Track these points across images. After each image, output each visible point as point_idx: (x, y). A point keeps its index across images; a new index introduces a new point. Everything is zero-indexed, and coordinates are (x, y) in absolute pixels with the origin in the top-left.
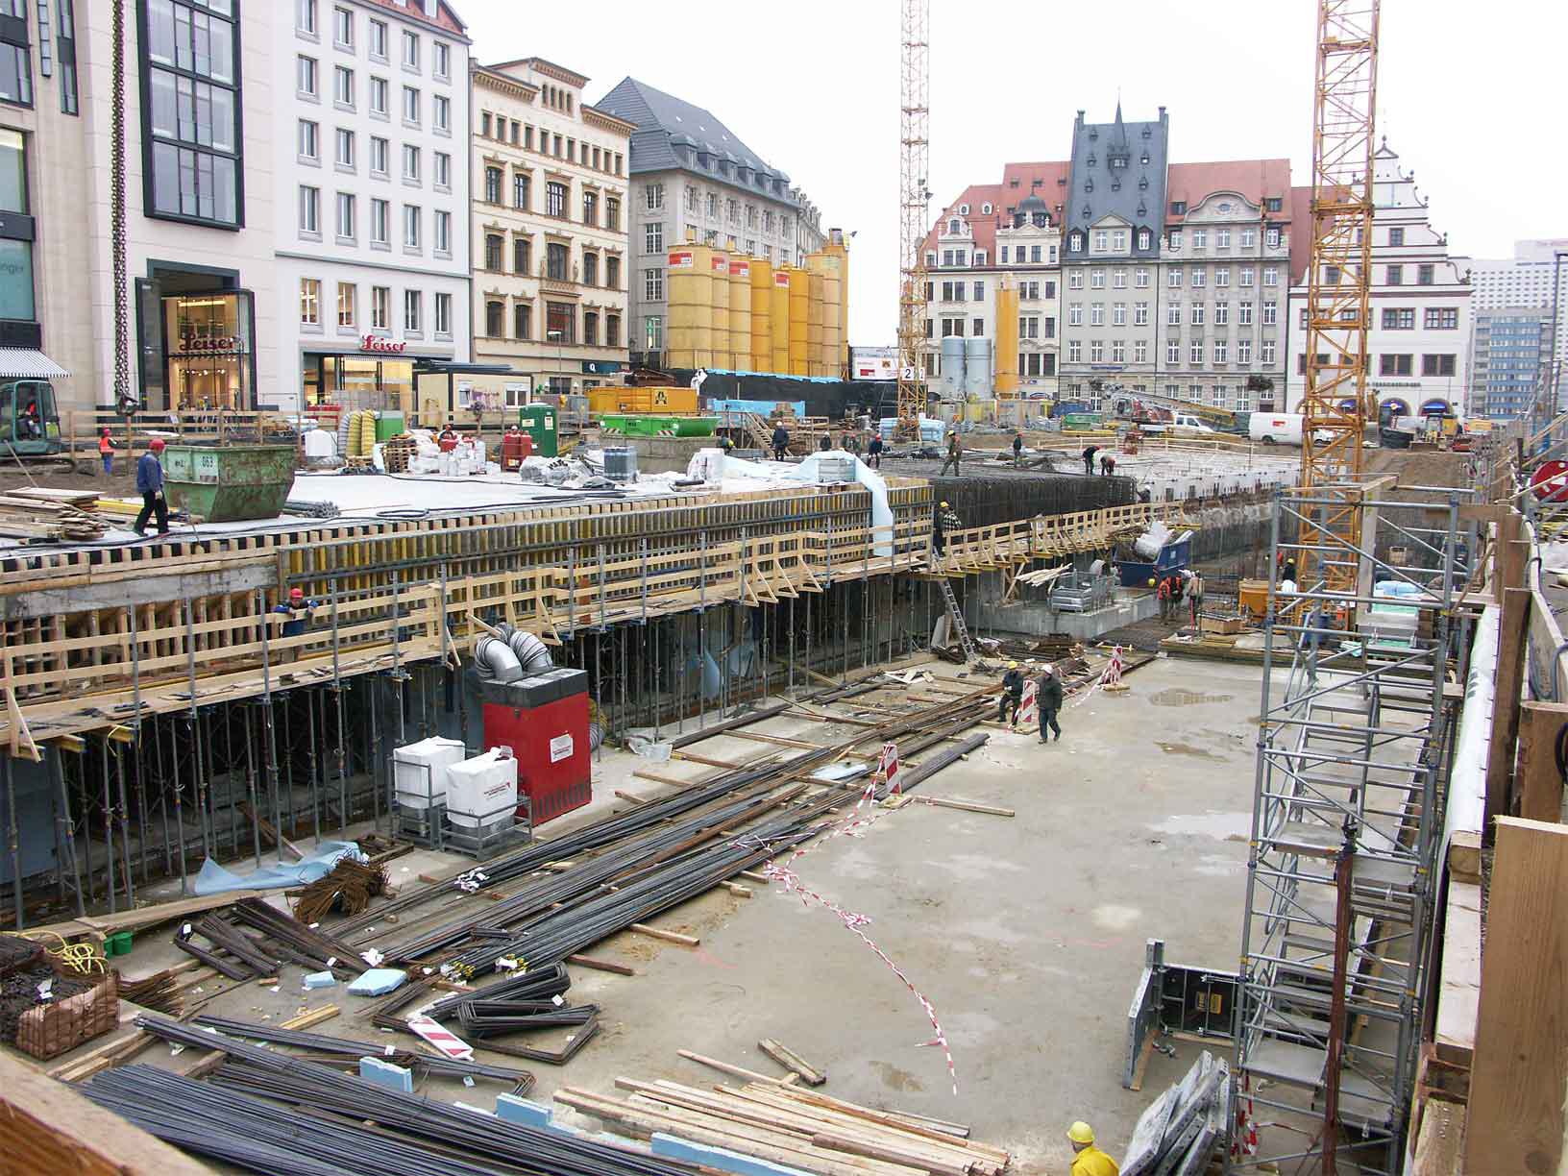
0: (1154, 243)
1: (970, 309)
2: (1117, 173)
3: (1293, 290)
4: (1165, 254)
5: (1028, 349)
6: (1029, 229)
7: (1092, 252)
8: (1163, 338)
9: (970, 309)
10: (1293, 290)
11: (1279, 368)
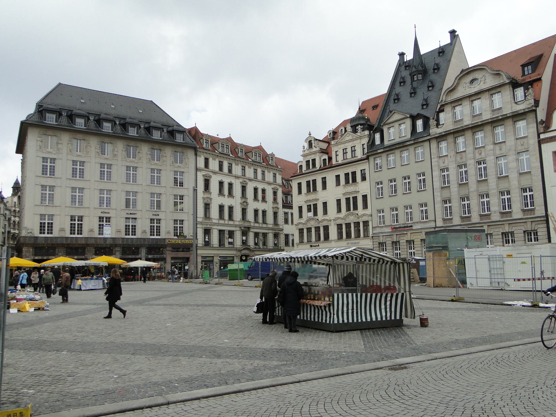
0: (426, 126)
2: (415, 84)
3: (542, 136)
4: (434, 131)
5: (352, 219)
6: (350, 136)
7: (386, 143)
8: (438, 199)
9: (321, 196)
10: (542, 136)
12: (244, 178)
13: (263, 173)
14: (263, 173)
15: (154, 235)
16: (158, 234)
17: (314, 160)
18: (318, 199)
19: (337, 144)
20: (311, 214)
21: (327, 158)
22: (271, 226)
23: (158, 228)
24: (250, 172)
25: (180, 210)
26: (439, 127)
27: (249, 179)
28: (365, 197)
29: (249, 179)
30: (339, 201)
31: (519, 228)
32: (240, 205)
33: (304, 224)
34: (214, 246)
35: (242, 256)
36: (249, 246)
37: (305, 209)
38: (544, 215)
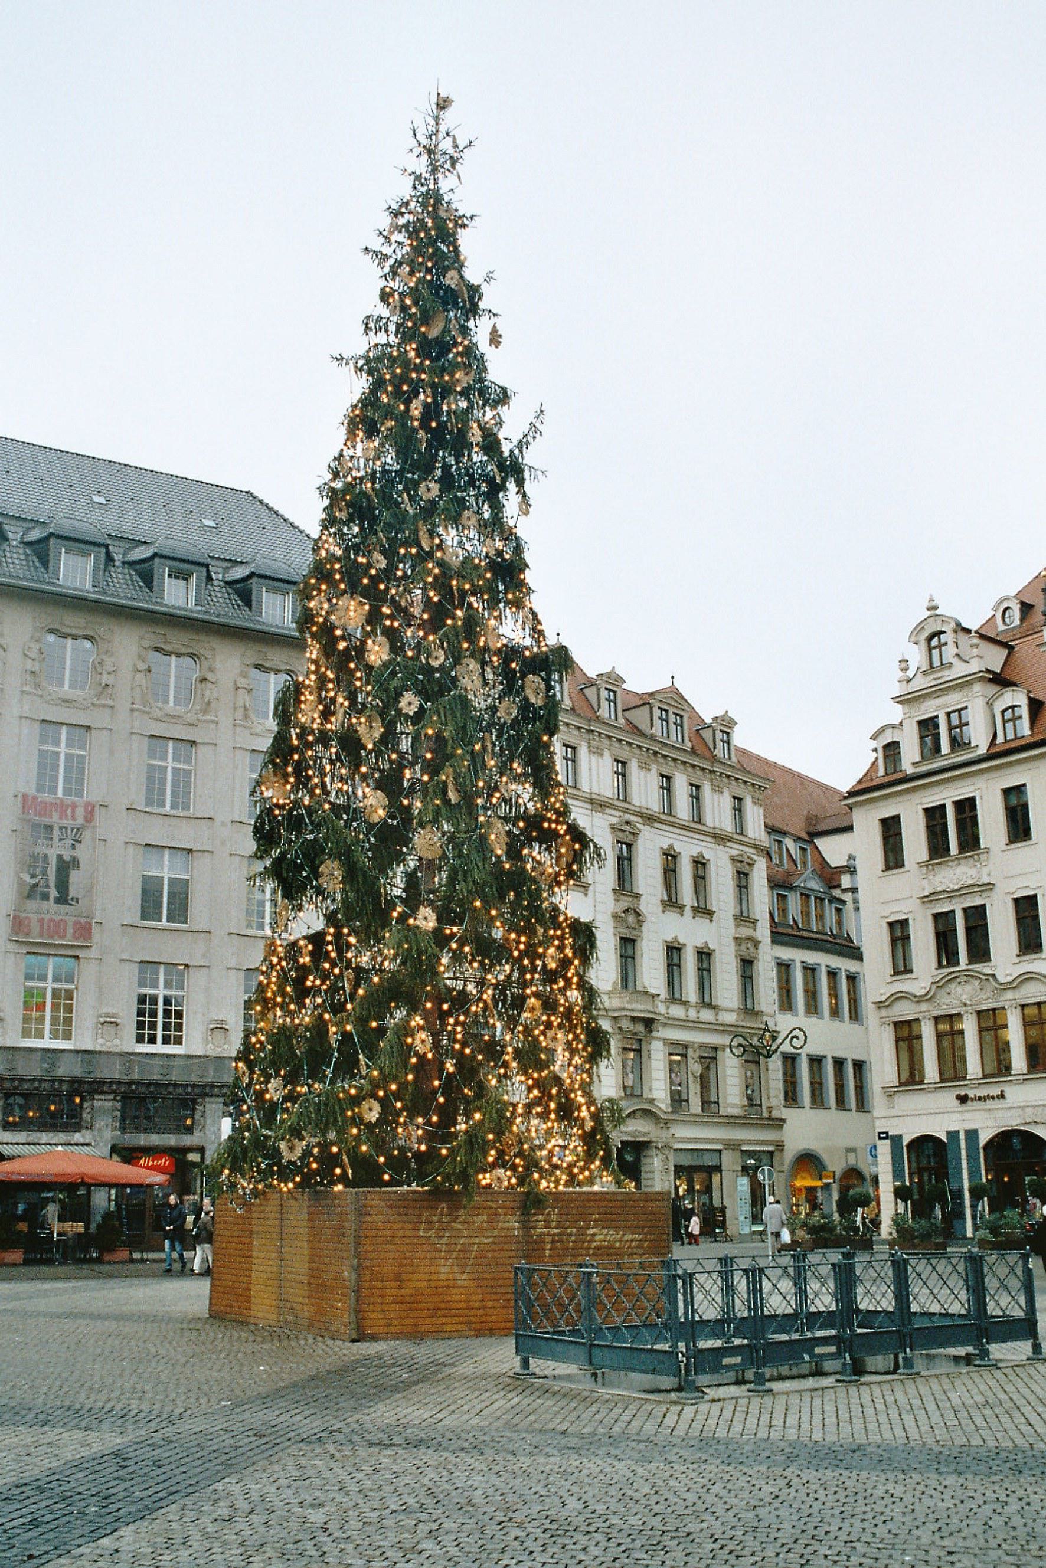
12: (625, 811)
13: (696, 797)
14: (696, 797)
18: (989, 887)
22: (730, 1018)
24: (645, 789)
27: (642, 815)
29: (642, 815)
32: (611, 923)
33: (919, 999)
36: (652, 1101)
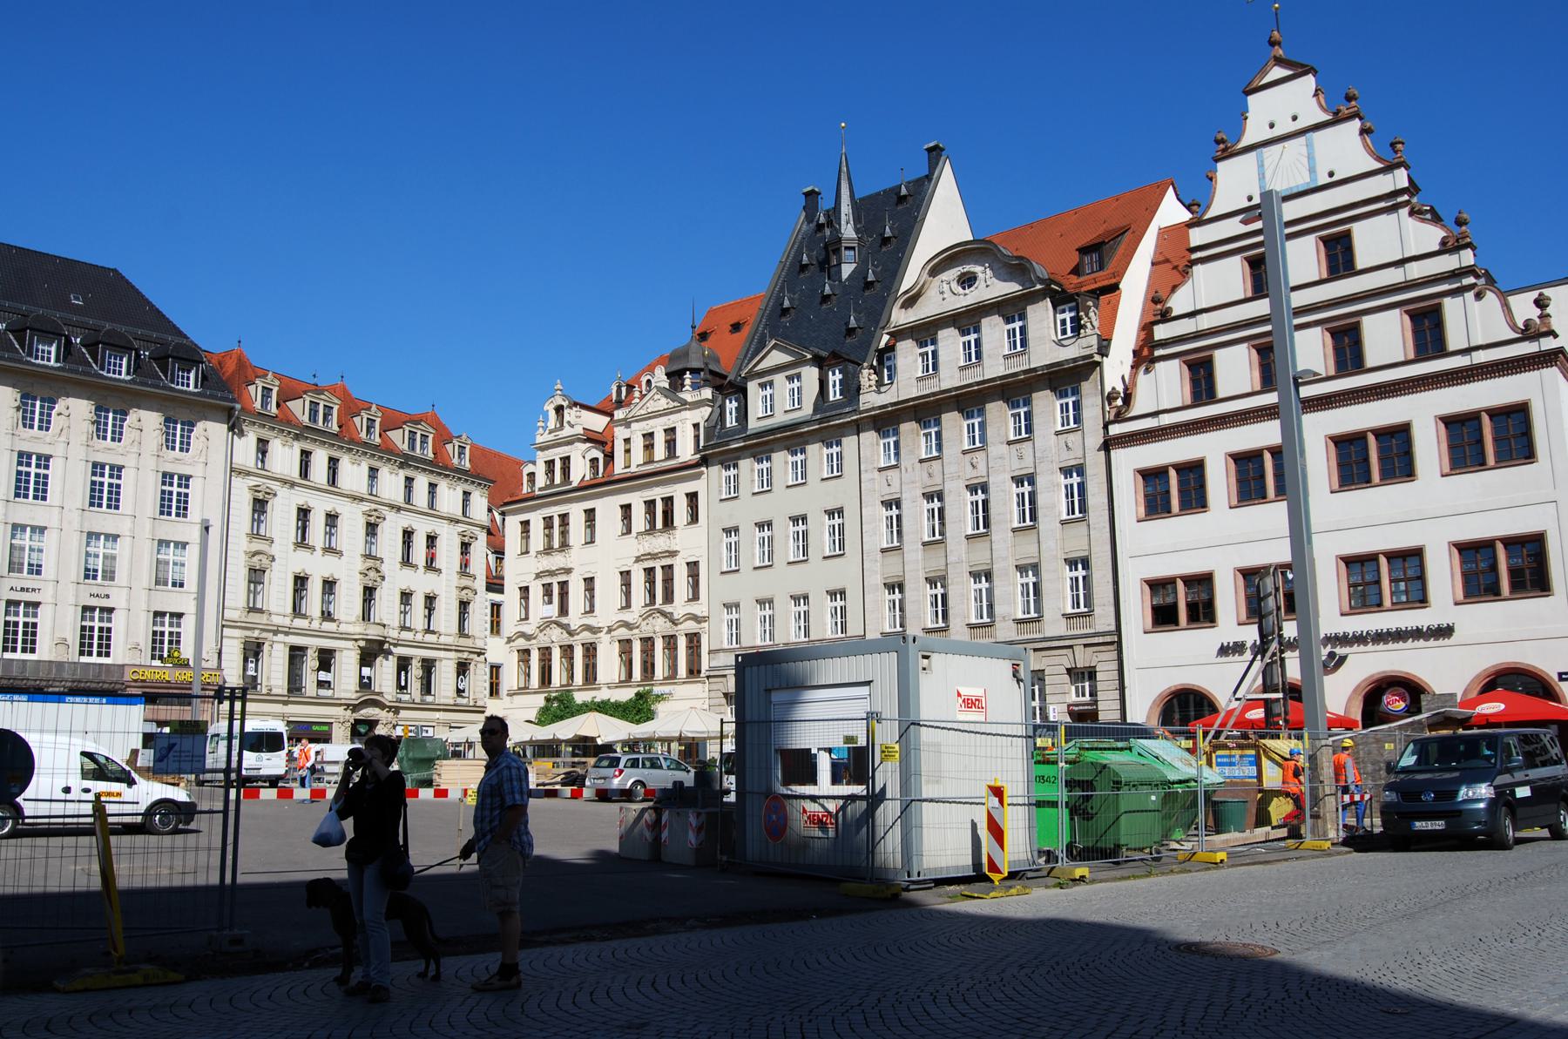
1: (580, 560)
3: (1115, 430)
4: (871, 400)
5: (659, 626)
7: (753, 425)
8: (876, 580)
9: (580, 560)
11: (1103, 620)
15: (90, 654)
16: (105, 650)
17: (566, 460)
19: (626, 423)
20: (553, 610)
21: (601, 456)
23: (106, 634)
25: (174, 584)
26: (883, 389)
28: (693, 567)
30: (626, 575)
31: (1056, 660)
34: (275, 691)
35: (357, 722)
37: (536, 593)
38: (1113, 628)
